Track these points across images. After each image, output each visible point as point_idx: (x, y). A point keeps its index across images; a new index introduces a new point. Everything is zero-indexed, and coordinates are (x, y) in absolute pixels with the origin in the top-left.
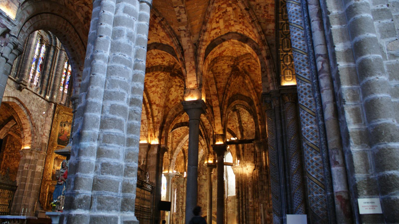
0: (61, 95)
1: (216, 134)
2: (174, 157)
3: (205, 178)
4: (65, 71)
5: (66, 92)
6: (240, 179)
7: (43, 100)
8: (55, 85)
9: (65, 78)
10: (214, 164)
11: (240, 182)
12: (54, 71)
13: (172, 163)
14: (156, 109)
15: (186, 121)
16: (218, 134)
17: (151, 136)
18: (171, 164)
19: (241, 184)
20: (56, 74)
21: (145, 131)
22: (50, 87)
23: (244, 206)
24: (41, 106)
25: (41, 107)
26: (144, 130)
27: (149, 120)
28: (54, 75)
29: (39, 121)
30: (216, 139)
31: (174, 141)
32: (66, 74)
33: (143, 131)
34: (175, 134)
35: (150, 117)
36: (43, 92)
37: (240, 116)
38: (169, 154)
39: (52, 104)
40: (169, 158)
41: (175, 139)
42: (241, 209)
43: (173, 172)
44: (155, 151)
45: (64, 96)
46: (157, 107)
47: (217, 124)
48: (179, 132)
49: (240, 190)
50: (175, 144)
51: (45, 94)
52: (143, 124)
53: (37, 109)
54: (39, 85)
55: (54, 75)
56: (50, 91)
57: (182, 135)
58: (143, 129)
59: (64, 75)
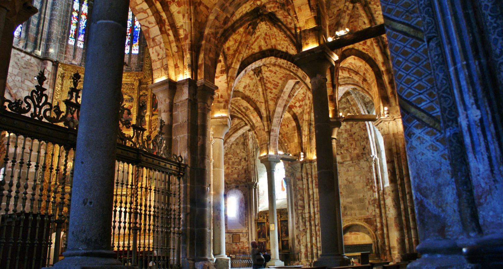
0: (72, 51)
1: (300, 32)
2: (275, 126)
3: (341, 161)
4: (75, 14)
5: (81, 45)
6: (393, 143)
7: (28, 57)
8: (50, 32)
9: (78, 24)
10: (335, 120)
11: (394, 150)
12: (48, 12)
13: (272, 138)
14: (179, 12)
15: (269, 47)
16: (305, 31)
17: (176, 66)
18: (271, 139)
19: (397, 153)
20: (52, 15)
21: (162, 59)
22: (42, 35)
23: (408, 197)
24: (25, 66)
25: (25, 68)
26: (160, 57)
27: (168, 35)
28: (48, 17)
29: (23, 90)
30: (303, 41)
31: (269, 98)
32: (79, 18)
33: (159, 59)
34: (268, 85)
35: (169, 30)
36: (31, 44)
37: (372, 14)
38: (265, 123)
39: (47, 63)
40: (266, 130)
41: (269, 94)
42: (401, 202)
43: (276, 153)
44: (185, 95)
45: (78, 52)
46: (179, 6)
47: (300, 9)
48: (273, 78)
49: (396, 165)
50: (271, 103)
51: (35, 48)
52: (157, 45)
53: (17, 71)
54: (23, 35)
55: (48, 17)
56: (43, 43)
57: (280, 85)
58: (158, 55)
59: (74, 21)
